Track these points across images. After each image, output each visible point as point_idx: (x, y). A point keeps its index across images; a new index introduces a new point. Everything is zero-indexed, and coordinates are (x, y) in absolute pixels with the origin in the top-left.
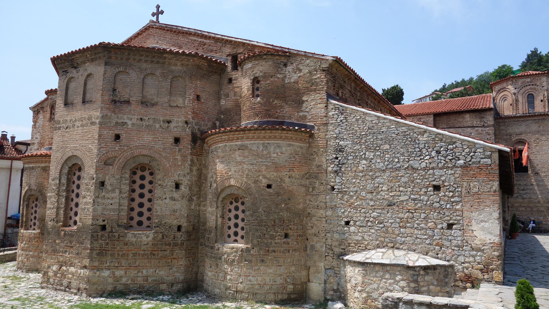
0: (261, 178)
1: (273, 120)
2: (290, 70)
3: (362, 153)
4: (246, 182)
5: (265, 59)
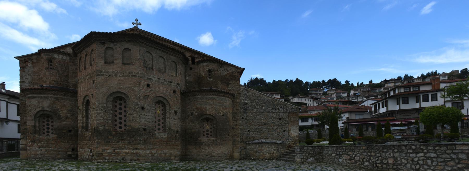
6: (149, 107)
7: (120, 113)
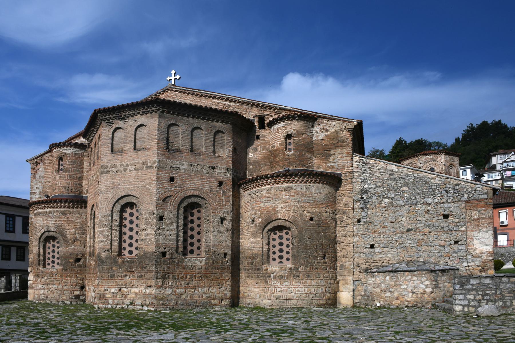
0: (305, 212)
1: (305, 169)
3: (384, 194)
4: (292, 216)
6: (173, 216)
7: (131, 229)
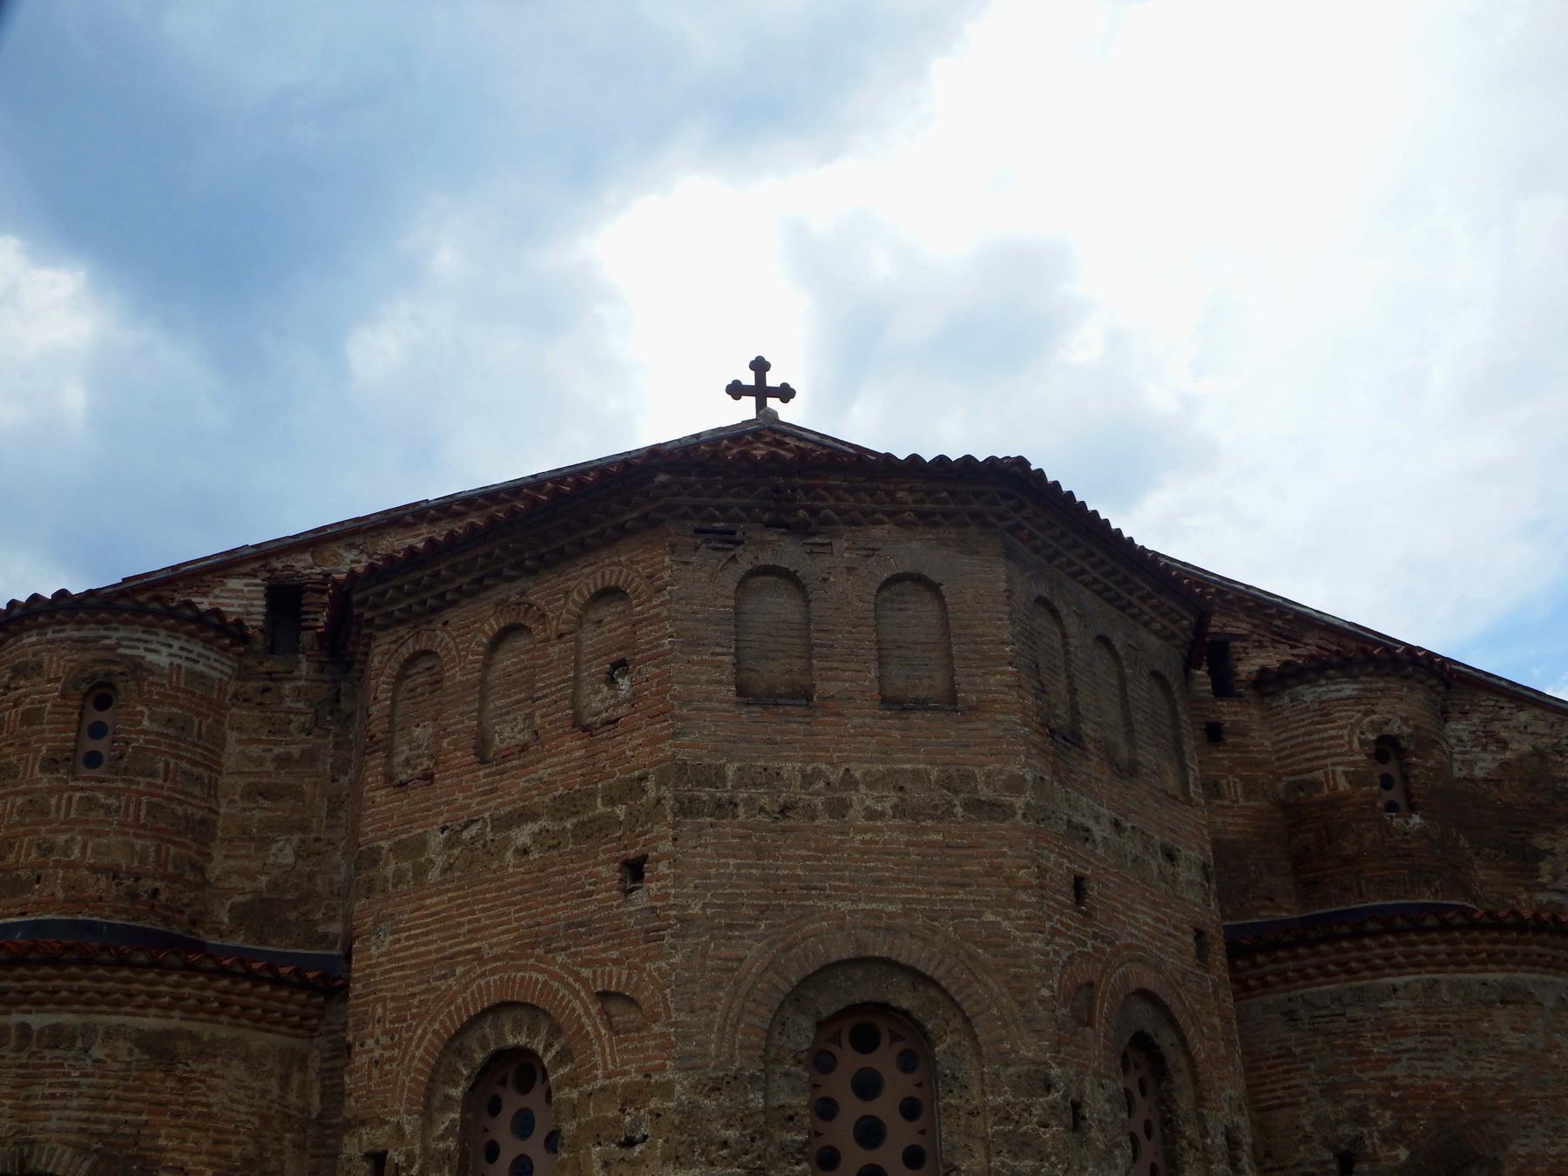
2: (1465, 736)
5: (1407, 677)
